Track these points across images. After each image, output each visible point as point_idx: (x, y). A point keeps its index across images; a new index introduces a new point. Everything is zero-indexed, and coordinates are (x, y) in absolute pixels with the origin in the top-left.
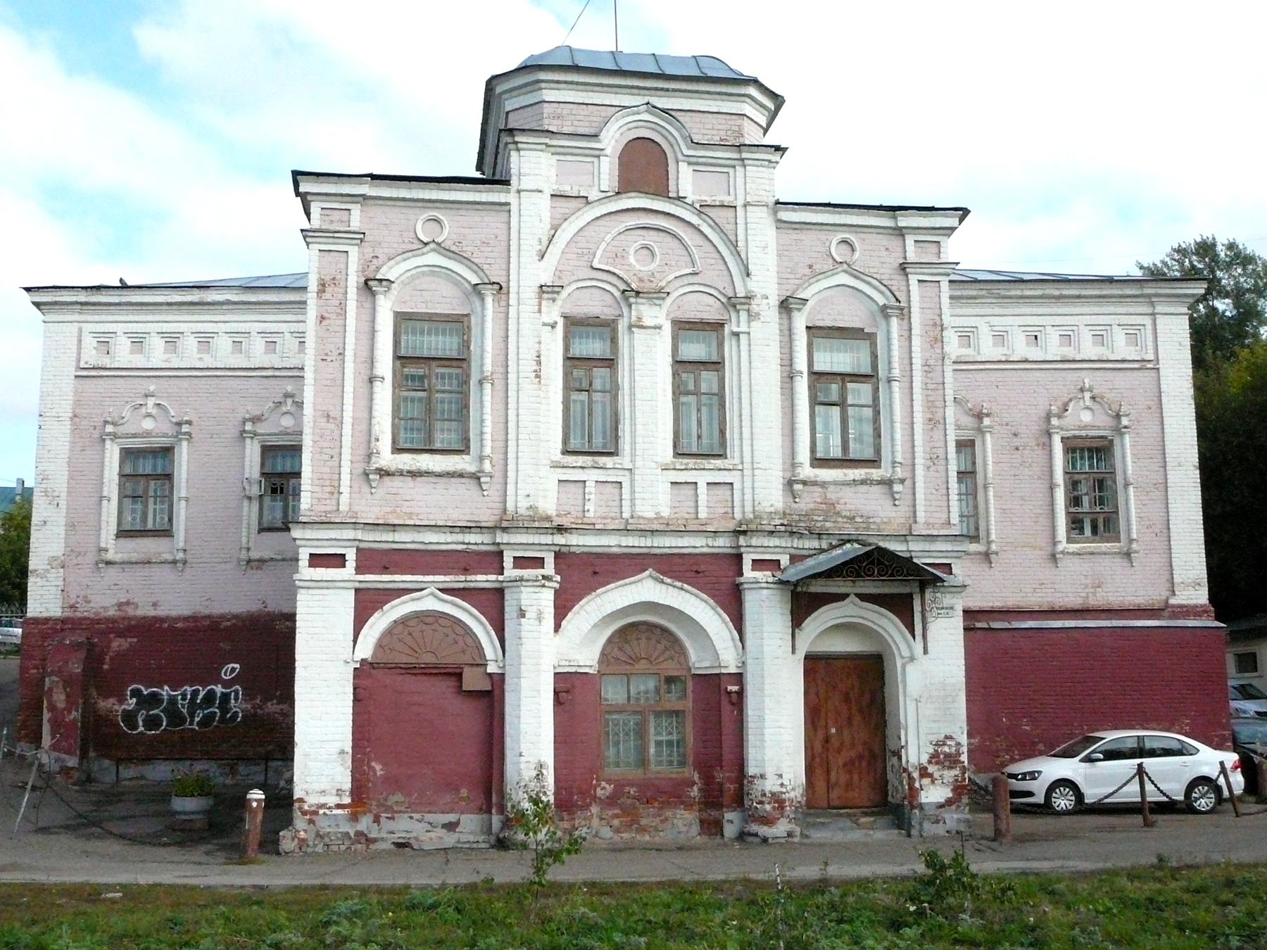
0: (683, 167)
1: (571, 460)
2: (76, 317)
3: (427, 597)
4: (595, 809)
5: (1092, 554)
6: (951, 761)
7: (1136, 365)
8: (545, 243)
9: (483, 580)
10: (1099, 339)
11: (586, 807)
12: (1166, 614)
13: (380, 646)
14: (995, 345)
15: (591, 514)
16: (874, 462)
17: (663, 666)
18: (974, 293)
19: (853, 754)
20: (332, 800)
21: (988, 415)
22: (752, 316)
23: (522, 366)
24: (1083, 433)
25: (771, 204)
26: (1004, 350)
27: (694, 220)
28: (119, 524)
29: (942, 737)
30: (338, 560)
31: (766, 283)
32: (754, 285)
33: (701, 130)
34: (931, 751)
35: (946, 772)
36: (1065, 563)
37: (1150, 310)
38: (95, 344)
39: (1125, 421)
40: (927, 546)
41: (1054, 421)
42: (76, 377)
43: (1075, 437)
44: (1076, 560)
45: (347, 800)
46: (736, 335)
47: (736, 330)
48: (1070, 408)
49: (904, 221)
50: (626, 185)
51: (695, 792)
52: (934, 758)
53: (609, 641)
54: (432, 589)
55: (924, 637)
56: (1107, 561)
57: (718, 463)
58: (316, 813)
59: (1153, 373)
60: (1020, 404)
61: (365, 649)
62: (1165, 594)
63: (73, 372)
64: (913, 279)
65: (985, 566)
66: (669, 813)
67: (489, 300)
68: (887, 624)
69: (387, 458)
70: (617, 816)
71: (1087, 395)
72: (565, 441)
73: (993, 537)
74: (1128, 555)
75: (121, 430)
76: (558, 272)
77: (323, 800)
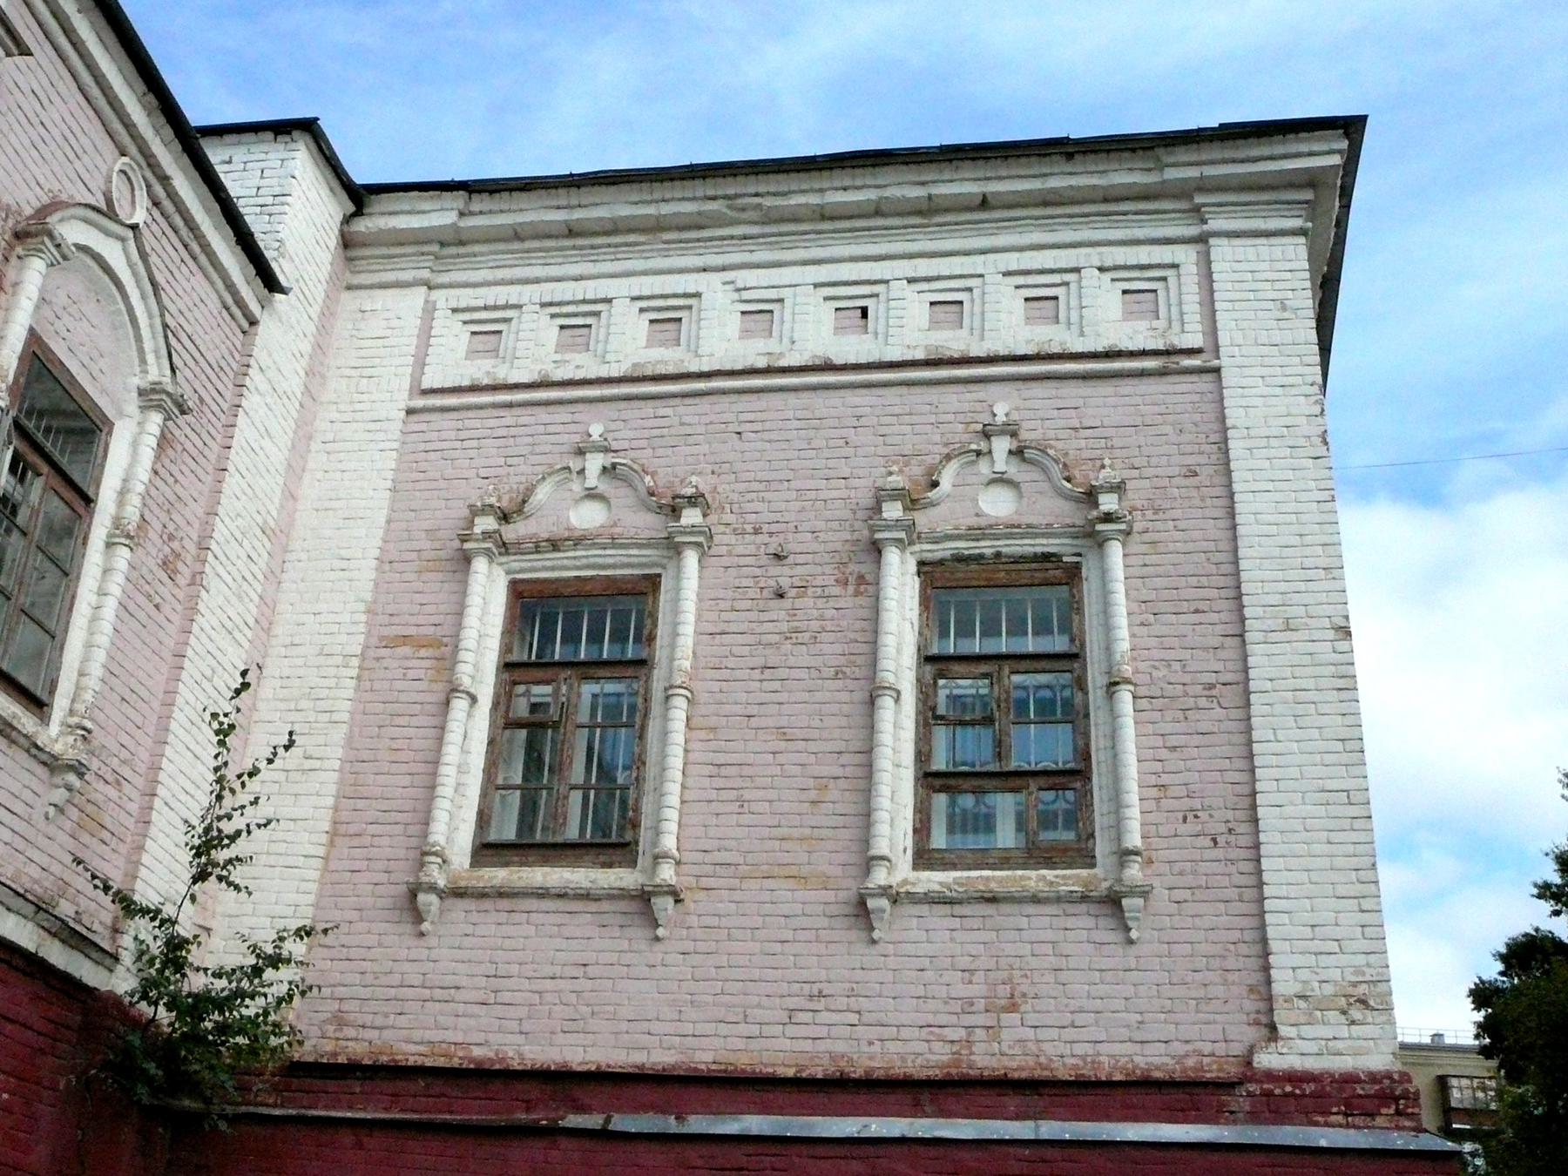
5: (993, 900)
10: (1042, 303)
12: (1239, 1102)
14: (746, 333)
21: (694, 500)
24: (986, 547)
26: (773, 345)
36: (896, 927)
37: (1193, 231)
39: (1108, 503)
41: (893, 511)
43: (959, 559)
44: (938, 918)
48: (947, 479)
56: (1041, 922)
59: (1204, 383)
60: (803, 472)
62: (1244, 1034)
65: (639, 933)
71: (1001, 445)
73: (669, 842)
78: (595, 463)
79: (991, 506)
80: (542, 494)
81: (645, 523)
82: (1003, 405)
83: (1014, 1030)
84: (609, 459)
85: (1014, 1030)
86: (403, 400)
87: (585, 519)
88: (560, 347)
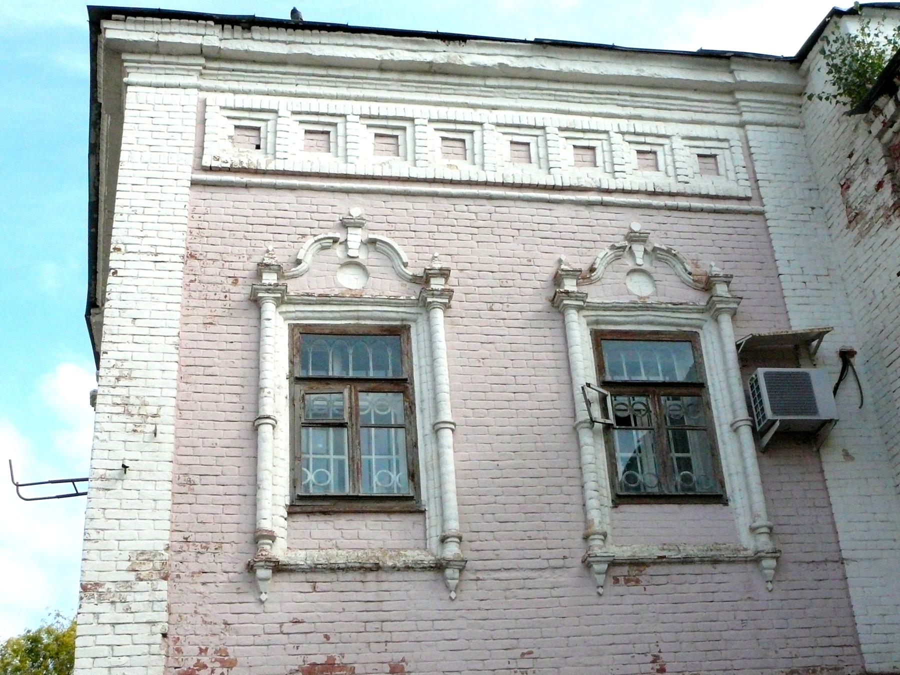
2: (194, 80)
28: (294, 483)
38: (232, 131)
42: (194, 183)
63: (188, 174)
75: (294, 287)
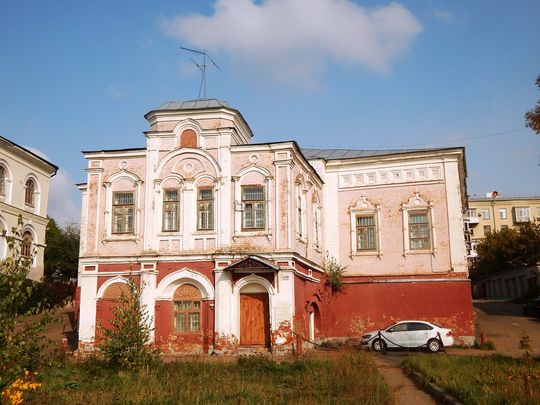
0: (201, 137)
1: (164, 234)
3: (119, 279)
4: (170, 344)
6: (287, 329)
7: (436, 182)
8: (157, 166)
9: (135, 272)
10: (422, 173)
11: (167, 343)
12: (448, 276)
13: (106, 293)
14: (382, 178)
15: (170, 250)
16: (263, 229)
17: (194, 298)
18: (373, 161)
19: (260, 327)
20: (89, 341)
22: (222, 184)
23: (149, 206)
24: (416, 209)
25: (229, 147)
26: (386, 180)
27: (204, 154)
29: (284, 321)
30: (93, 268)
31: (227, 173)
32: (223, 174)
33: (205, 125)
34: (279, 326)
35: (285, 333)
37: (442, 161)
39: (431, 204)
40: (278, 256)
41: (404, 205)
45: (94, 341)
46: (217, 190)
47: (217, 188)
48: (410, 200)
49: (274, 147)
50: (183, 145)
51: (202, 339)
52: (281, 328)
53: (177, 290)
54: (119, 275)
55: (278, 287)
57: (210, 232)
58: (84, 345)
61: (101, 295)
64: (277, 166)
66: (193, 345)
67: (139, 185)
68: (265, 282)
69: (110, 236)
70: (177, 346)
71: (417, 195)
72: (163, 228)
73: (381, 249)
74: (378, 256)
76: (161, 175)
77: (86, 341)
78: (364, 198)
79: (417, 203)
80: (358, 203)
81: (373, 207)
82: (417, 189)
83: (422, 268)
84: (366, 198)
85: (422, 268)
86: (337, 190)
87: (364, 207)
88: (358, 181)
